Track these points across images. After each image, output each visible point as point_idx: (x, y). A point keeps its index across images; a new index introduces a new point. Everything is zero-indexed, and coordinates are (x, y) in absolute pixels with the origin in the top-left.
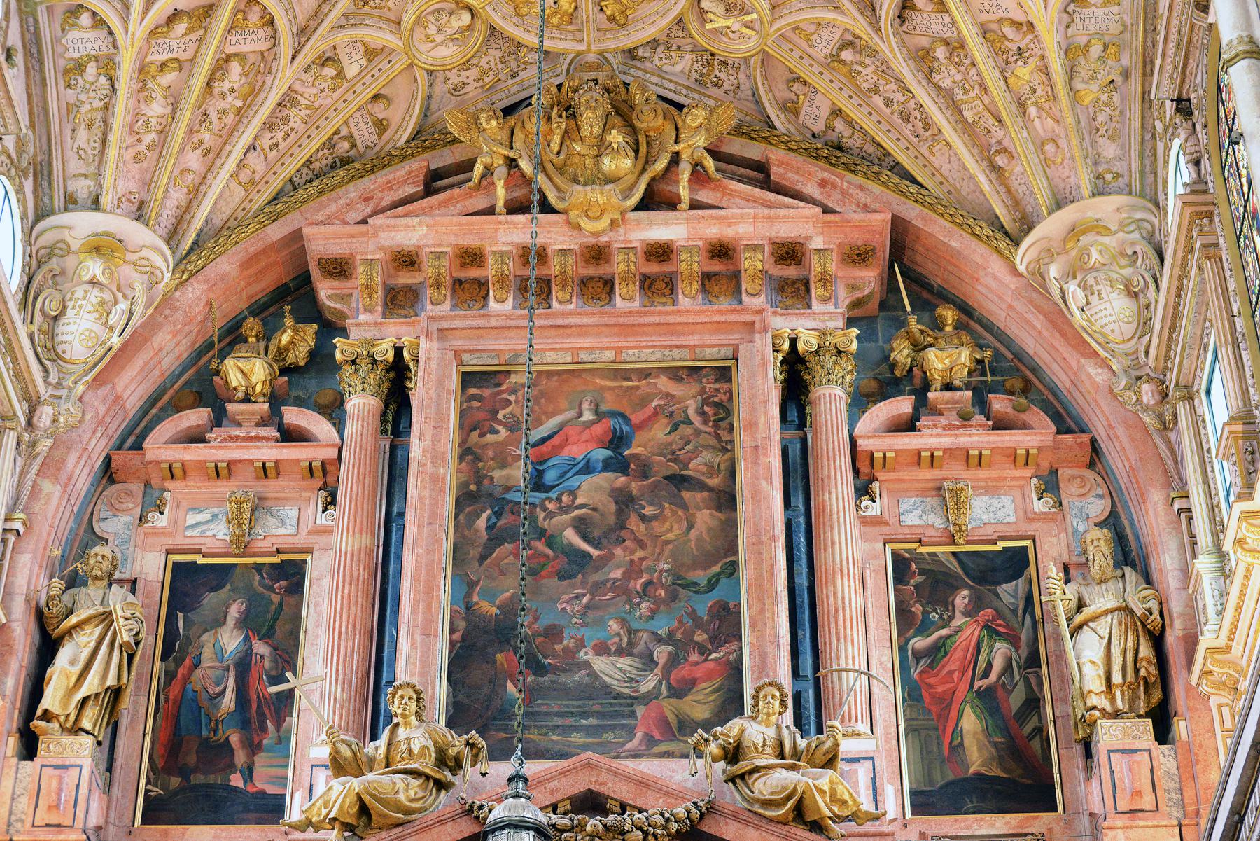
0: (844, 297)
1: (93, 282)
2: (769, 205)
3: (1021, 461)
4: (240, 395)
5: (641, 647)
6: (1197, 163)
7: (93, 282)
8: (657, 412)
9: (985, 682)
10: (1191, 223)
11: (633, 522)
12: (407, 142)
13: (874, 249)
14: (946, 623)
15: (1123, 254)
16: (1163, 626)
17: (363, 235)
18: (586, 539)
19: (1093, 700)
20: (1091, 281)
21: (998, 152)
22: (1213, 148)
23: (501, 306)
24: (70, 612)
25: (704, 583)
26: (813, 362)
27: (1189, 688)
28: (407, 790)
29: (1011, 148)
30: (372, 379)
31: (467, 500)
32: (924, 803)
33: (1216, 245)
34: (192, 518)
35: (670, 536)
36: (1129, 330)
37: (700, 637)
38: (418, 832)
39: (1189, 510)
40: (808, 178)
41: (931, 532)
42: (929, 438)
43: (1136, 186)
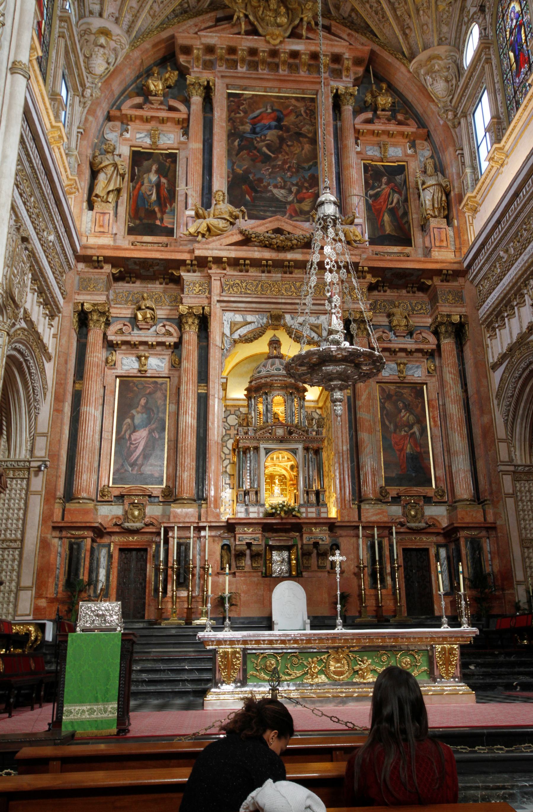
0: (353, 76)
1: (102, 46)
2: (331, 40)
3: (405, 136)
4: (154, 93)
5: (287, 187)
6: (485, 29)
7: (102, 46)
8: (292, 111)
9: (391, 206)
10: (482, 51)
11: (285, 147)
12: (208, 6)
13: (364, 60)
14: (379, 187)
15: (445, 68)
16: (450, 191)
17: (195, 38)
18: (270, 151)
19: (429, 212)
20: (434, 76)
21: (407, 28)
22: (494, 23)
23: (242, 69)
24: (101, 163)
25: (307, 168)
26: (342, 97)
27: (458, 210)
28: (221, 224)
29: (412, 26)
30: (199, 91)
31: (232, 135)
32: (372, 242)
33: (490, 59)
34: (138, 136)
35: (296, 152)
36: (445, 93)
37: (306, 185)
38: (225, 238)
39: (463, 154)
40: (345, 33)
41: (376, 158)
42: (377, 127)
43: (453, 43)
